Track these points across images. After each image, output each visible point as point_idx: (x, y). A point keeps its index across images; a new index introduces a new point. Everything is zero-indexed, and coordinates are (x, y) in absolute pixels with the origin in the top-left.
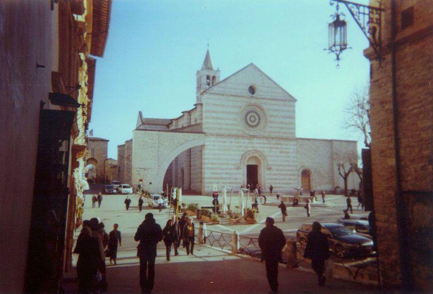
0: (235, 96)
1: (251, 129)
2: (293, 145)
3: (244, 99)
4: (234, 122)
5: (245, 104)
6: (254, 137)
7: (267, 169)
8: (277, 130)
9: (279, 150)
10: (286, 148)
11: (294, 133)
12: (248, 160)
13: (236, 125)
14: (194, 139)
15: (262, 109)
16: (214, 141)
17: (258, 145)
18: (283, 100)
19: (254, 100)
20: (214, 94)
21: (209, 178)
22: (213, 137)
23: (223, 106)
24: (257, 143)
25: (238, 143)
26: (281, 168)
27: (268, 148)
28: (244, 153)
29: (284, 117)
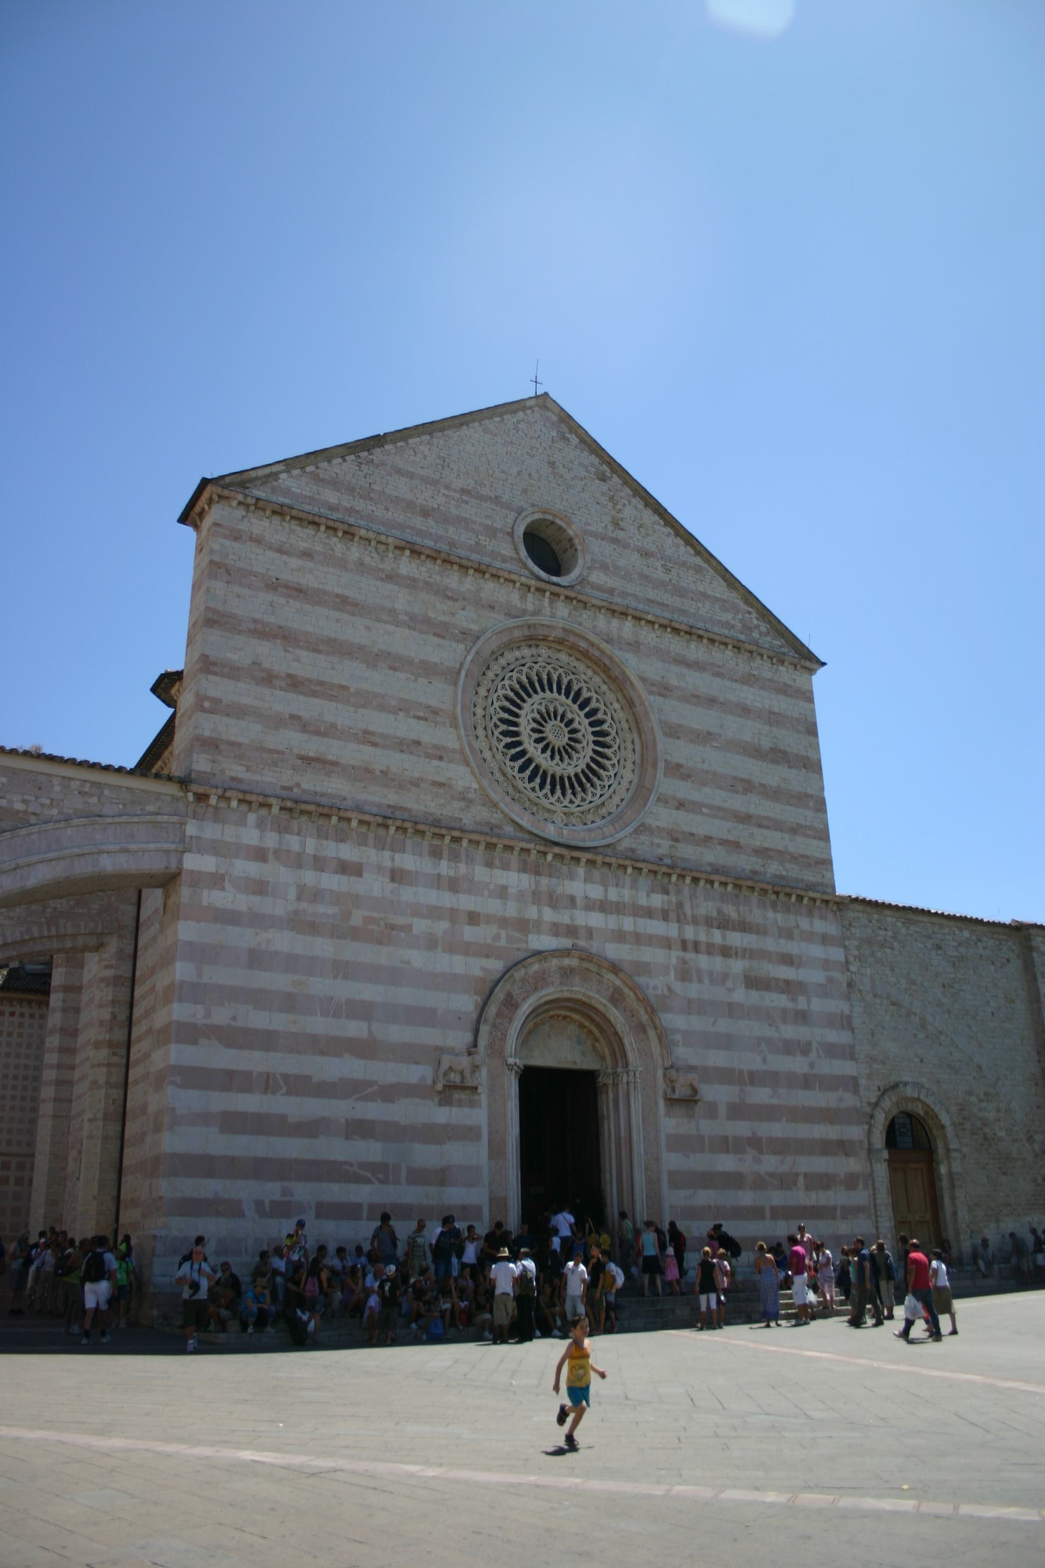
1: (544, 798)
2: (825, 940)
4: (428, 734)
5: (512, 622)
7: (671, 1102)
8: (720, 828)
9: (738, 966)
10: (787, 960)
11: (827, 863)
12: (527, 1036)
13: (439, 754)
14: (91, 816)
15: (617, 681)
16: (260, 855)
17: (596, 920)
18: (737, 648)
19: (562, 610)
20: (280, 512)
22: (252, 817)
23: (343, 603)
24: (591, 906)
25: (453, 885)
26: (761, 1095)
27: (666, 943)
28: (497, 966)
29: (756, 752)
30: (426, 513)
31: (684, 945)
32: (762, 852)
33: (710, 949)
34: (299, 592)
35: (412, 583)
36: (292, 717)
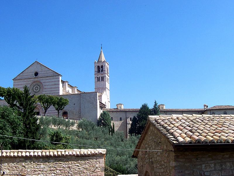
3: (31, 80)
15: (41, 83)
29: (53, 85)
30: (27, 75)
34: (18, 85)
35: (26, 81)
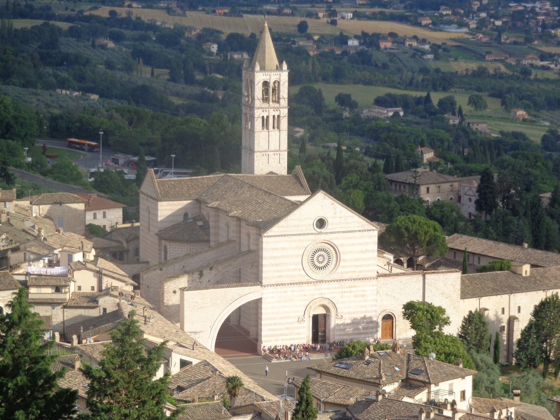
0: (299, 235)
1: (318, 271)
6: (321, 281)
9: (353, 294)
10: (364, 291)
16: (273, 293)
18: (360, 231)
20: (273, 236)
21: (267, 336)
23: (284, 249)
25: (302, 291)
27: (339, 293)
29: (362, 252)
30: (298, 226)
31: (342, 292)
32: (361, 272)
33: (347, 292)
34: (277, 249)
36: (277, 270)
